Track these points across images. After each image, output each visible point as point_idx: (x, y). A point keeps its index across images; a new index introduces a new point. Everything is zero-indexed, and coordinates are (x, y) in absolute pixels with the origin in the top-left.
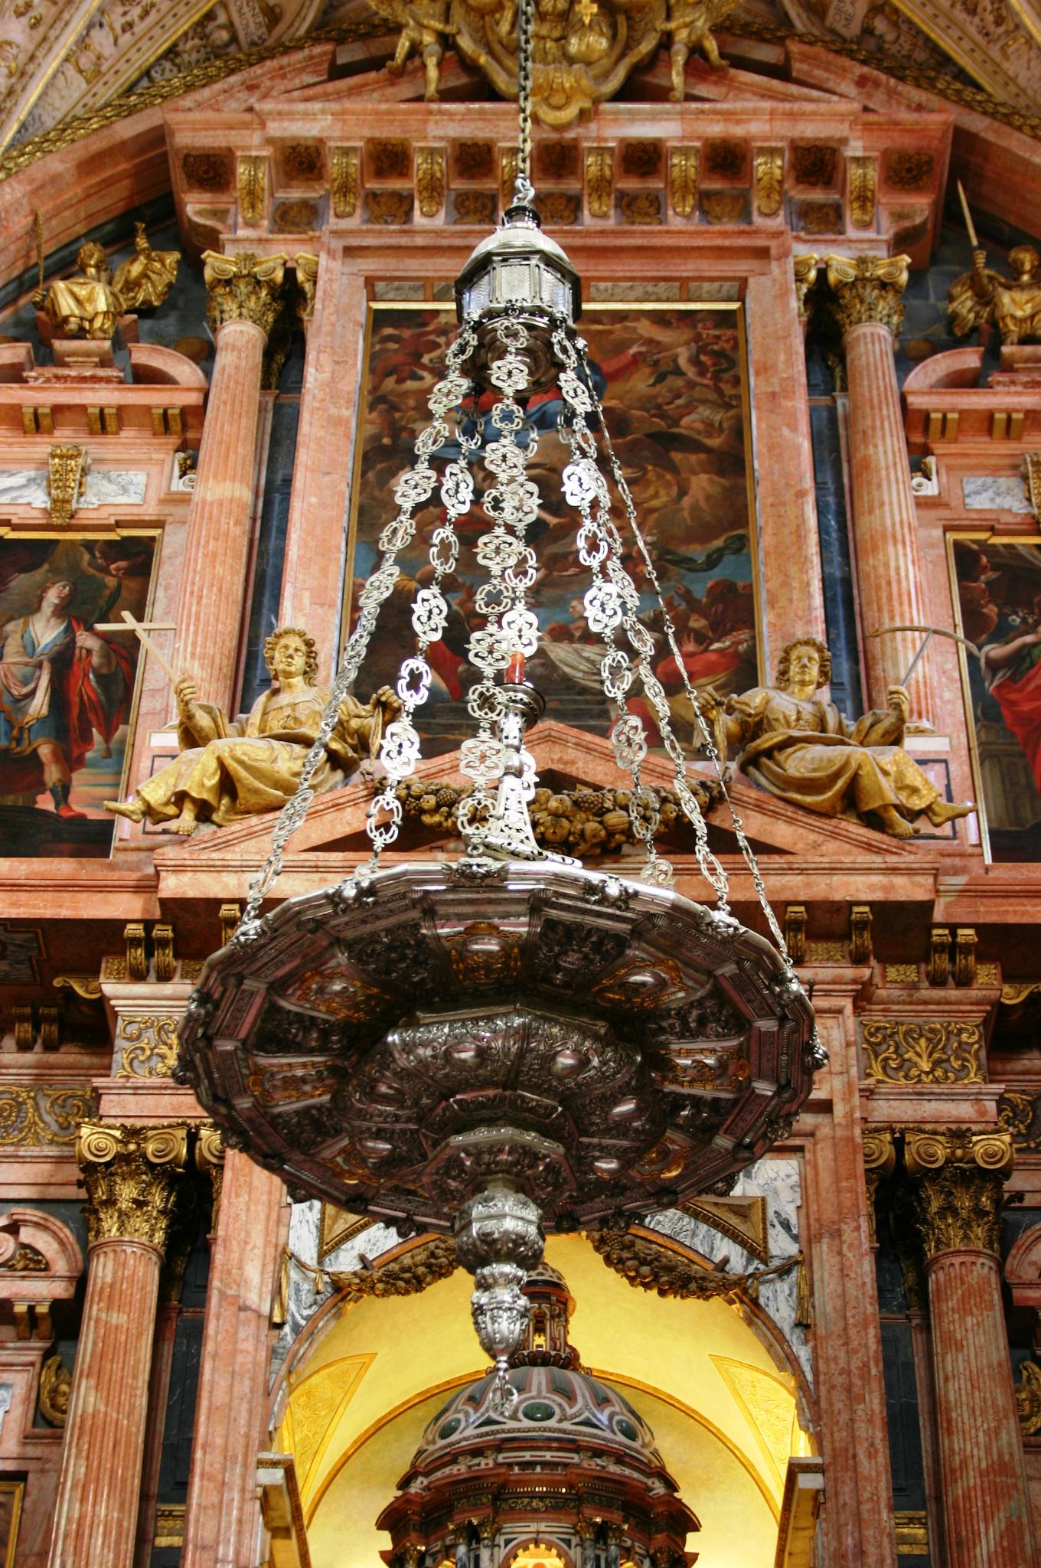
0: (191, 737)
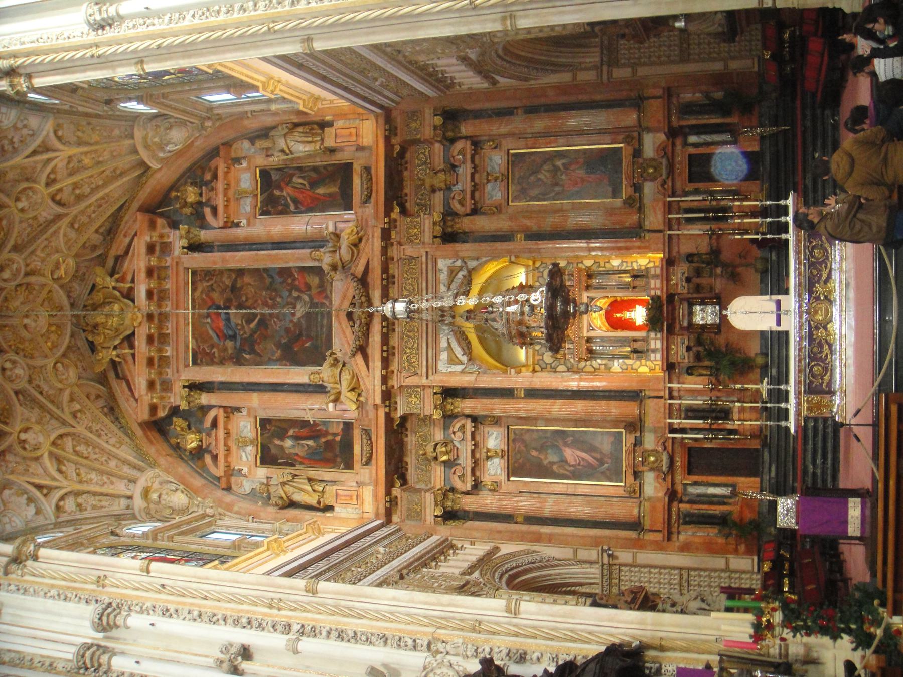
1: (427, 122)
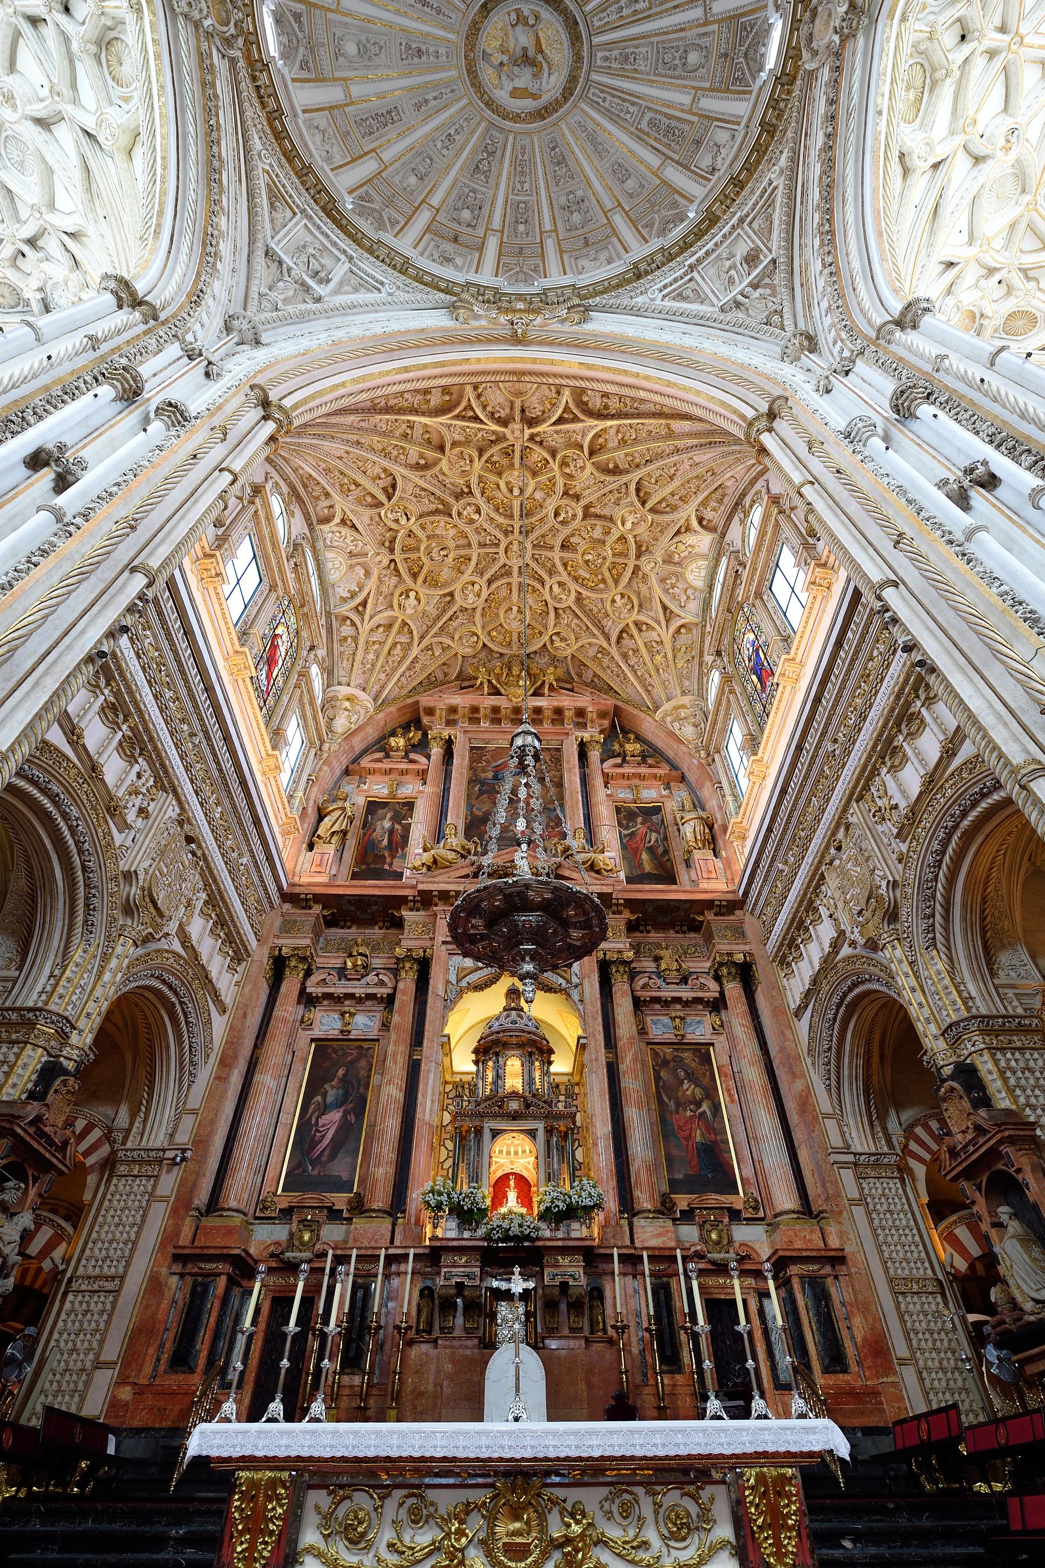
0: (425, 850)
1: (735, 947)
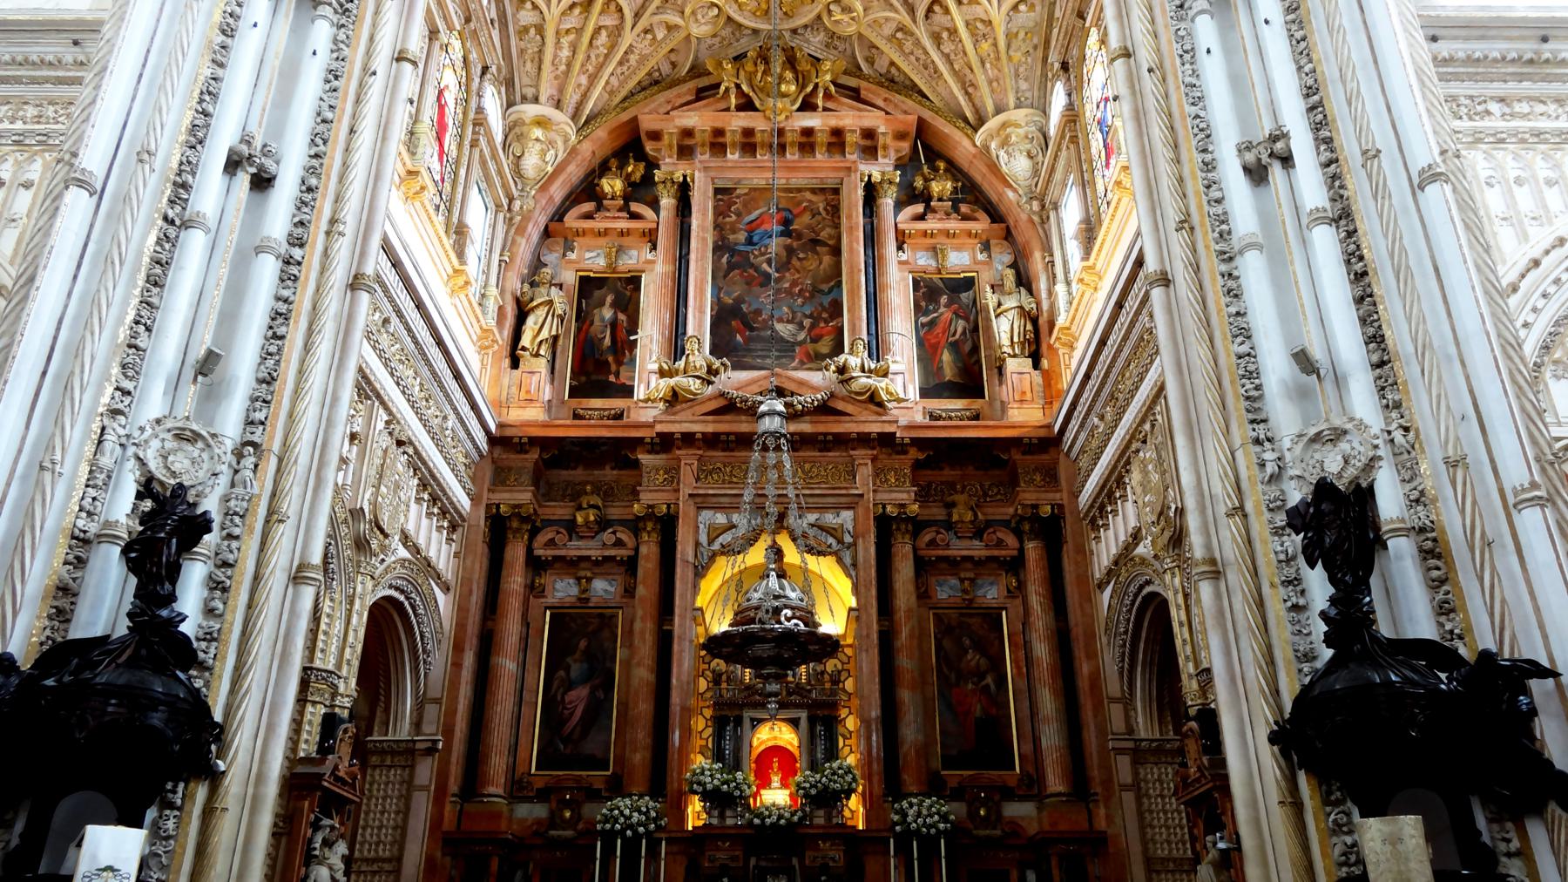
1: (1043, 496)
